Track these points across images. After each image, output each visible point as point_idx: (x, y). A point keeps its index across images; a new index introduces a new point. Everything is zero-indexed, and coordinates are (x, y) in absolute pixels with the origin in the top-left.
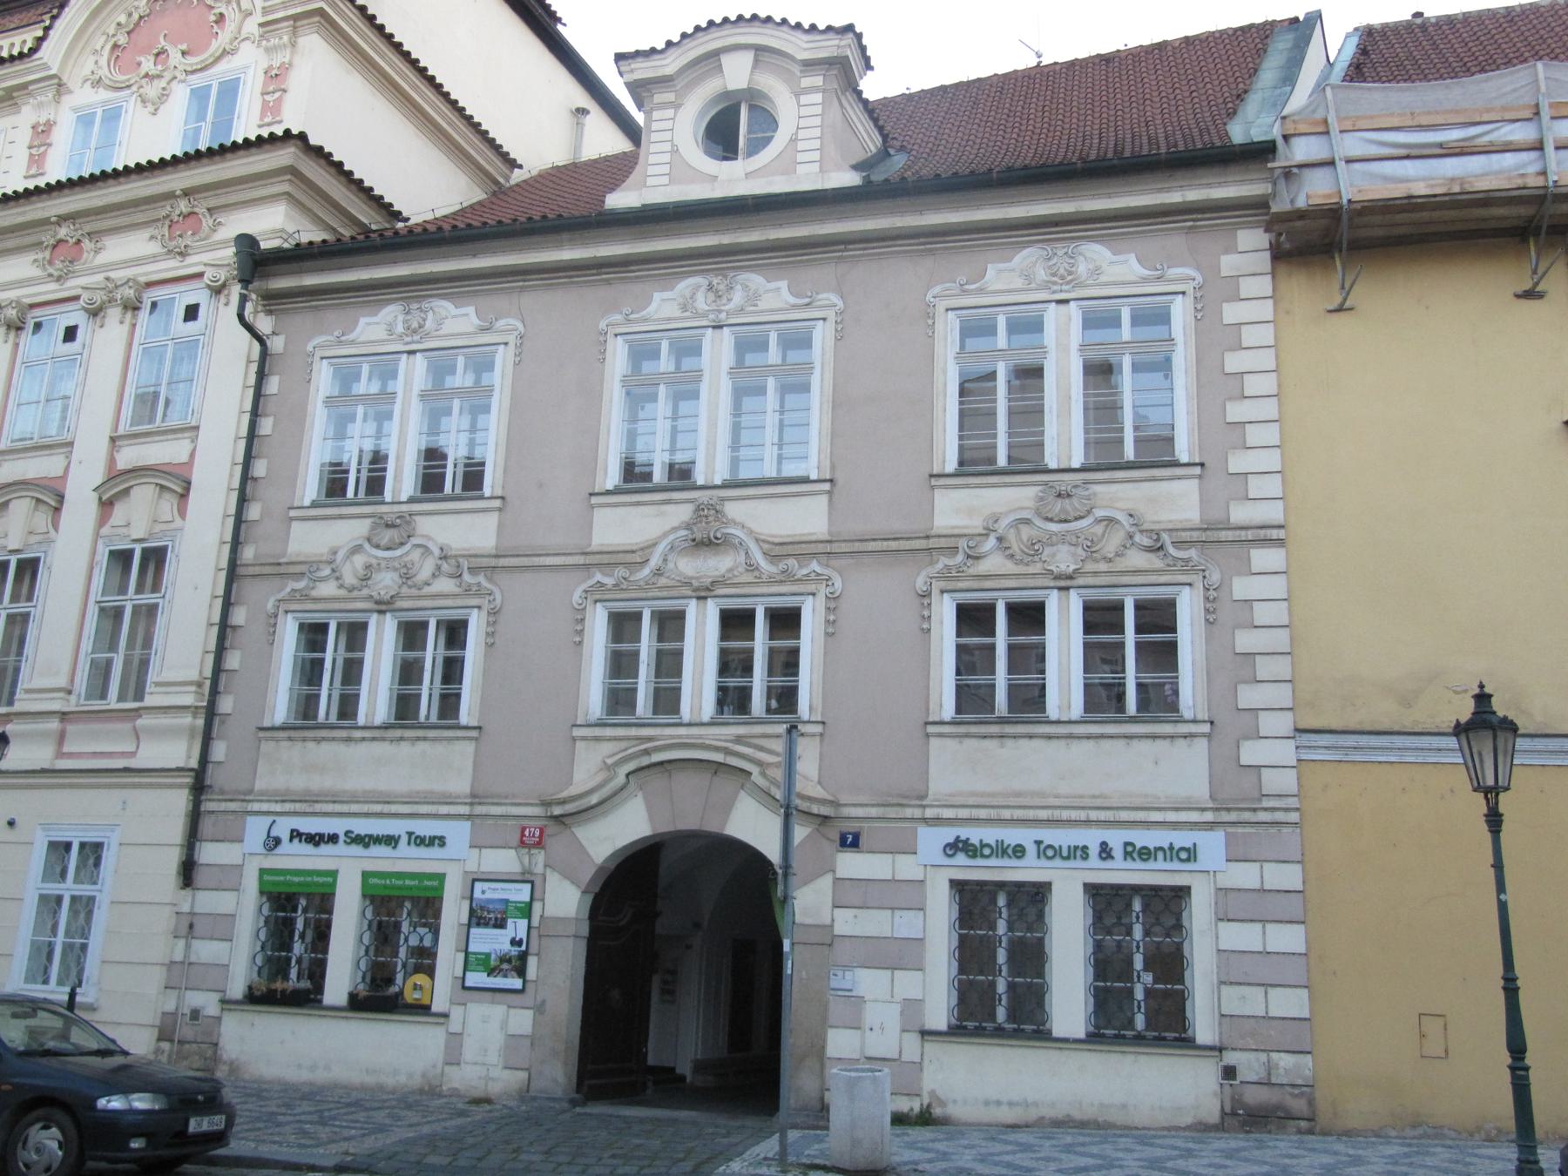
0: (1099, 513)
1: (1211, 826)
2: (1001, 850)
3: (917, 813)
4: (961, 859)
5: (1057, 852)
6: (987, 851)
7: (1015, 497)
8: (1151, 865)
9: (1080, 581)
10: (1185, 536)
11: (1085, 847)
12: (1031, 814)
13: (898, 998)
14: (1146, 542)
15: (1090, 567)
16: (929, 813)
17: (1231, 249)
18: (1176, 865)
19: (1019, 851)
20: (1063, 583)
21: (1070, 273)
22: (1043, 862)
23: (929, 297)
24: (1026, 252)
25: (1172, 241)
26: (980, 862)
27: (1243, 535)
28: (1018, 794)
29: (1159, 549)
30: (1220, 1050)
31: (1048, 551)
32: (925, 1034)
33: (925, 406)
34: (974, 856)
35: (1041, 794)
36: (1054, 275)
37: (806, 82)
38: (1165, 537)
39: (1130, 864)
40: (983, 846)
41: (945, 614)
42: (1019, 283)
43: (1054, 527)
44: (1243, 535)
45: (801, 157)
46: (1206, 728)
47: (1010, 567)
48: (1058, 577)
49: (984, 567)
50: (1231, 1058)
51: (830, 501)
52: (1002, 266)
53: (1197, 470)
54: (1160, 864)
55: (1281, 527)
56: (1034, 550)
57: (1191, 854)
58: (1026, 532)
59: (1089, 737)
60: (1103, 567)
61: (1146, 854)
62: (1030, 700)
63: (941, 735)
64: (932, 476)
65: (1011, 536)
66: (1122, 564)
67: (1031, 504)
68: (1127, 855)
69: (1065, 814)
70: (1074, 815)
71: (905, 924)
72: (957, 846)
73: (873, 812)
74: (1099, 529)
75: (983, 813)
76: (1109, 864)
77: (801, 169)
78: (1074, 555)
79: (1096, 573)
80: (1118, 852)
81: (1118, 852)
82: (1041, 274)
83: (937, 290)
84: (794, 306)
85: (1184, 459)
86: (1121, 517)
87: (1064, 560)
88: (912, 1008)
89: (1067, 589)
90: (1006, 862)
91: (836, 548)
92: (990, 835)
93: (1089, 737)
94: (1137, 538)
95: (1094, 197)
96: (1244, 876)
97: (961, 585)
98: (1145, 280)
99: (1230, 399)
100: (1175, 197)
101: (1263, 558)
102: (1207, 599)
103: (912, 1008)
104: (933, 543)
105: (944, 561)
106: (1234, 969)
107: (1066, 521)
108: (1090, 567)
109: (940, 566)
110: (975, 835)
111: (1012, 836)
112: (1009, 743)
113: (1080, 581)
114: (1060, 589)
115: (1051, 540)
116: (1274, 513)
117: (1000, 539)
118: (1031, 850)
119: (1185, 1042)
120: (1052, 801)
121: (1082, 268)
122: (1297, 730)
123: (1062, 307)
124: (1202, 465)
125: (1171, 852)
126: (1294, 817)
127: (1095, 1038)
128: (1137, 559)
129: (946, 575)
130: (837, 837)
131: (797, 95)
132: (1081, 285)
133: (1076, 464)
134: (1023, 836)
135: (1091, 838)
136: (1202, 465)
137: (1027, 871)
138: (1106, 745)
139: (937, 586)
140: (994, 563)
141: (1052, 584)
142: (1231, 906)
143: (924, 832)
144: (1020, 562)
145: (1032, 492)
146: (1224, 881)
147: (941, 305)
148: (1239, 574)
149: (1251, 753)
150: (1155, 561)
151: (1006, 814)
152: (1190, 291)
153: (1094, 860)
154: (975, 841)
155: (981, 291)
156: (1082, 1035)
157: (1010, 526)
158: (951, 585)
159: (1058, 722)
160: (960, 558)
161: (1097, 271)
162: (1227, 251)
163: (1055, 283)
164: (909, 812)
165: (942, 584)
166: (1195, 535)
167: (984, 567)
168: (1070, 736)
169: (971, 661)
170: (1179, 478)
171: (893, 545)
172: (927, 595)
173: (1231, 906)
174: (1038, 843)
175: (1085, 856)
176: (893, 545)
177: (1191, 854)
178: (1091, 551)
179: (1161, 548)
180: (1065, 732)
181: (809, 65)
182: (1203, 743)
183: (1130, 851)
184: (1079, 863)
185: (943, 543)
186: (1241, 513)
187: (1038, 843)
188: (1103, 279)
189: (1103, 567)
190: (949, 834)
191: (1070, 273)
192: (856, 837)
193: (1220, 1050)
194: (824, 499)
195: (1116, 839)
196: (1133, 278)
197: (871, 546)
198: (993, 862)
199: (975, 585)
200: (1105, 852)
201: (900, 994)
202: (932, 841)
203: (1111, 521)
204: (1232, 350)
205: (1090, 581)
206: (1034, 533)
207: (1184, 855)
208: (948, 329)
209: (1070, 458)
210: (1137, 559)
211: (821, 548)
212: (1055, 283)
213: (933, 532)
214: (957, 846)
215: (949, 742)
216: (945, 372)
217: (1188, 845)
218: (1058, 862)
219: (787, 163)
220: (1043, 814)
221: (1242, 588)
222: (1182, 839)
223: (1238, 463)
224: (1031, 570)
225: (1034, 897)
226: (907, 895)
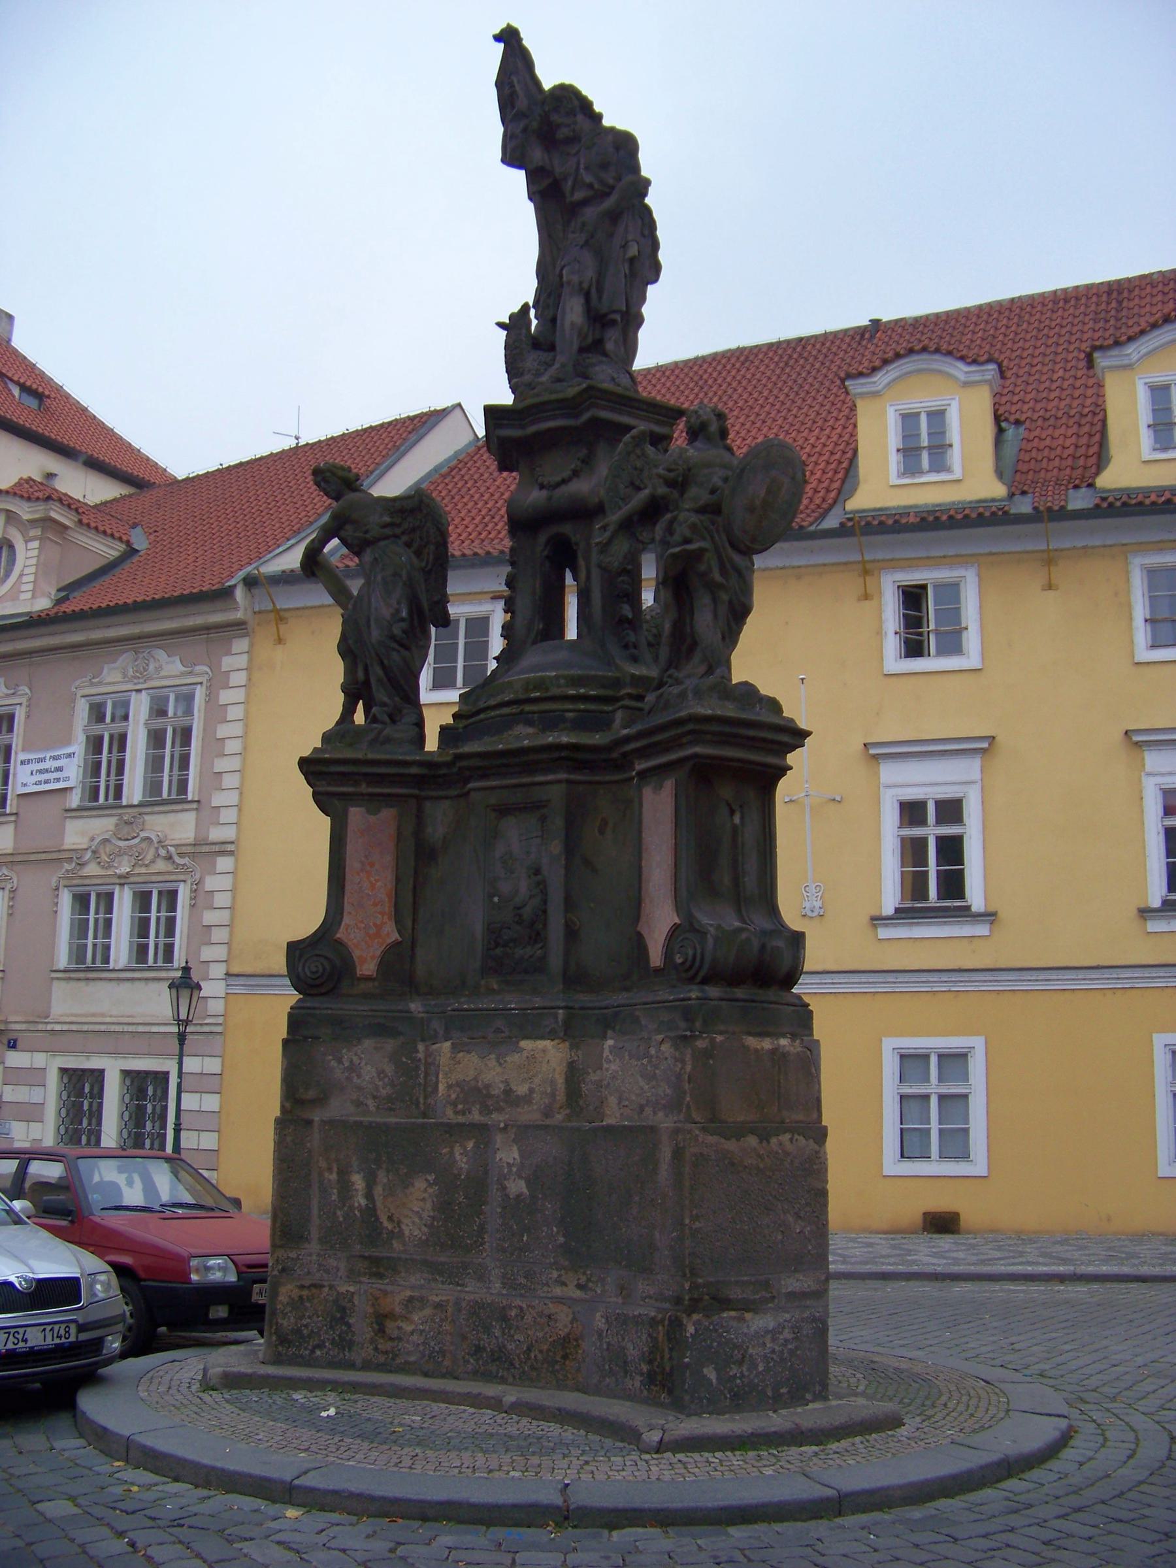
0: (143, 834)
7: (102, 825)
10: (184, 849)
13: (30, 1138)
15: (138, 870)
17: (229, 653)
20: (123, 881)
24: (125, 655)
28: (93, 1015)
29: (169, 858)
35: (103, 1015)
36: (137, 671)
37: (32, 533)
38: (172, 849)
41: (66, 900)
42: (119, 677)
43: (122, 844)
45: (24, 588)
48: (120, 877)
51: (16, 828)
55: (232, 843)
58: (108, 848)
59: (128, 979)
60: (143, 870)
63: (58, 979)
67: (112, 828)
71: (36, 1095)
73: (24, 1027)
74: (144, 845)
77: (23, 596)
78: (129, 861)
82: (131, 673)
83: (77, 683)
84: (7, 696)
91: (20, 858)
93: (128, 979)
97: (75, 882)
98: (183, 674)
99: (217, 756)
100: (190, 622)
101: (224, 863)
105: (67, 866)
107: (128, 840)
108: (138, 870)
109: (64, 870)
112: (92, 983)
113: (132, 879)
115: (121, 853)
116: (228, 833)
117: (94, 852)
120: (108, 1020)
121: (151, 667)
122: (227, 974)
124: (198, 801)
126: (219, 1029)
128: (161, 866)
130: (6, 1042)
131: (26, 542)
132: (150, 679)
138: (137, 983)
140: (92, 869)
141: (117, 881)
144: (103, 867)
147: (79, 695)
148: (209, 874)
150: (170, 868)
152: (205, 682)
155: (100, 683)
160: (74, 864)
161: (159, 669)
162: (226, 655)
163: (135, 677)
166: (190, 849)
170: (187, 810)
171: (43, 856)
172: (57, 889)
176: (43, 856)
180: (120, 977)
181: (33, 522)
185: (66, 855)
186: (216, 834)
188: (163, 673)
192: (15, 1041)
194: (11, 827)
197: (33, 857)
203: (148, 838)
208: (82, 710)
210: (161, 866)
211: (10, 859)
213: (63, 848)
215: (63, 984)
219: (13, 595)
220: (103, 1028)
223: (218, 800)
226: (34, 1077)
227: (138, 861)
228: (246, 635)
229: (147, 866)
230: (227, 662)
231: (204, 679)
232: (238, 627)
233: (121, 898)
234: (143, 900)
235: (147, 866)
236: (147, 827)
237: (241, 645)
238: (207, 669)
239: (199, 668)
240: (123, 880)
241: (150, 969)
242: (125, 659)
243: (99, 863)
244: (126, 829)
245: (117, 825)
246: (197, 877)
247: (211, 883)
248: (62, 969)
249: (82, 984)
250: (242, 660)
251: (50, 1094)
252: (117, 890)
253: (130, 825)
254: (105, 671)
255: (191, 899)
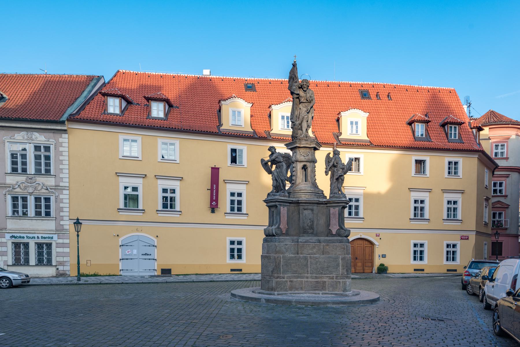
0: (37, 182)
1: (56, 234)
2: (20, 237)
3: (5, 231)
4: (13, 239)
5: (30, 238)
6: (18, 237)
8: (46, 239)
9: (34, 194)
10: (52, 187)
11: (35, 237)
12: (25, 232)
14: (45, 188)
15: (35, 191)
16: (7, 231)
17: (61, 137)
18: (50, 240)
19: (23, 237)
20: (30, 194)
21: (31, 138)
22: (28, 239)
23: (4, 139)
24: (23, 132)
25: (51, 135)
26: (16, 239)
27: (62, 188)
28: (23, 229)
30: (56, 266)
31: (28, 188)
32: (8, 265)
33: (4, 160)
34: (16, 238)
39: (42, 239)
40: (17, 237)
41: (9, 198)
42: (22, 138)
44: (62, 188)
46: (55, 219)
47: (21, 191)
48: (29, 193)
49: (16, 190)
50: (57, 267)
52: (18, 134)
53: (54, 176)
54: (47, 239)
56: (26, 188)
57: (52, 238)
58: (24, 185)
59: (35, 220)
60: (38, 192)
61: (45, 238)
62: (25, 214)
64: (5, 173)
65: (21, 185)
66: (41, 191)
67: (25, 180)
68: (41, 238)
69: (31, 232)
70: (33, 232)
72: (12, 237)
74: (37, 185)
75: (17, 232)
76: (39, 239)
78: (32, 189)
79: (36, 193)
80: (40, 238)
81: (40, 238)
82: (26, 137)
83: (5, 137)
85: (52, 174)
86: (40, 183)
87: (31, 190)
88: (5, 262)
89: (31, 195)
90: (21, 239)
92: (18, 235)
93: (35, 220)
94: (43, 187)
95: (34, 125)
96: (61, 241)
99: (60, 164)
101: (65, 192)
102: (55, 198)
103: (5, 262)
104: (6, 186)
105: (8, 189)
106: (58, 255)
110: (16, 235)
111: (22, 235)
113: (34, 194)
114: (30, 195)
116: (67, 185)
117: (19, 186)
118: (26, 237)
119: (51, 265)
121: (34, 137)
123: (30, 144)
124: (55, 176)
125: (49, 238)
126: (68, 232)
127: (37, 265)
128: (44, 191)
129: (9, 191)
132: (33, 140)
133: (33, 173)
134: (25, 235)
135: (36, 235)
136: (55, 176)
137: (25, 240)
139: (7, 193)
140: (18, 190)
142: (59, 245)
143: (6, 234)
144: (22, 190)
145: (25, 177)
146: (57, 242)
147: (6, 141)
149: (62, 223)
150: (47, 191)
151: (21, 232)
152: (54, 144)
153: (36, 239)
154: (16, 236)
155: (14, 139)
156: (35, 265)
157: (21, 183)
158: (10, 193)
159: (30, 217)
160: (11, 188)
161: (37, 138)
163: (28, 139)
164: (3, 231)
165: (8, 193)
166: (54, 187)
167: (16, 190)
168: (32, 219)
169: (15, 206)
172: (5, 195)
173: (59, 245)
174: (27, 236)
175: (35, 238)
177: (52, 238)
178: (36, 189)
179: (48, 189)
180: (31, 219)
182: (54, 221)
183: (42, 237)
184: (34, 239)
186: (61, 184)
187: (27, 236)
188: (38, 140)
189: (38, 192)
190: (11, 235)
191: (31, 138)
193: (56, 266)
195: (40, 236)
196: (43, 140)
198: (19, 239)
199: (14, 193)
200: (38, 237)
201: (3, 260)
202: (8, 236)
204: (61, 156)
205: (35, 194)
206: (25, 185)
207: (51, 238)
209: (32, 172)
210: (44, 191)
212: (28, 139)
214: (12, 237)
216: (7, 154)
217: (52, 236)
218: (30, 239)
221: (61, 196)
222: (51, 236)
223: (61, 175)
224: (25, 191)
225: (26, 245)
227: (36, 189)
228: (67, 133)
229: (39, 191)
230: (61, 140)
231: (53, 143)
232: (65, 131)
233: (30, 199)
234: (38, 200)
235: (39, 191)
236: (37, 180)
237: (66, 136)
238: (54, 141)
239: (51, 140)
240: (31, 194)
241: (43, 217)
242: (23, 133)
243: (21, 189)
244: (30, 180)
245: (26, 179)
246: (57, 195)
247: (61, 196)
248: (10, 216)
249: (18, 220)
250: (67, 140)
251: (10, 249)
252: (29, 197)
253: (30, 179)
254: (16, 135)
255: (55, 200)
